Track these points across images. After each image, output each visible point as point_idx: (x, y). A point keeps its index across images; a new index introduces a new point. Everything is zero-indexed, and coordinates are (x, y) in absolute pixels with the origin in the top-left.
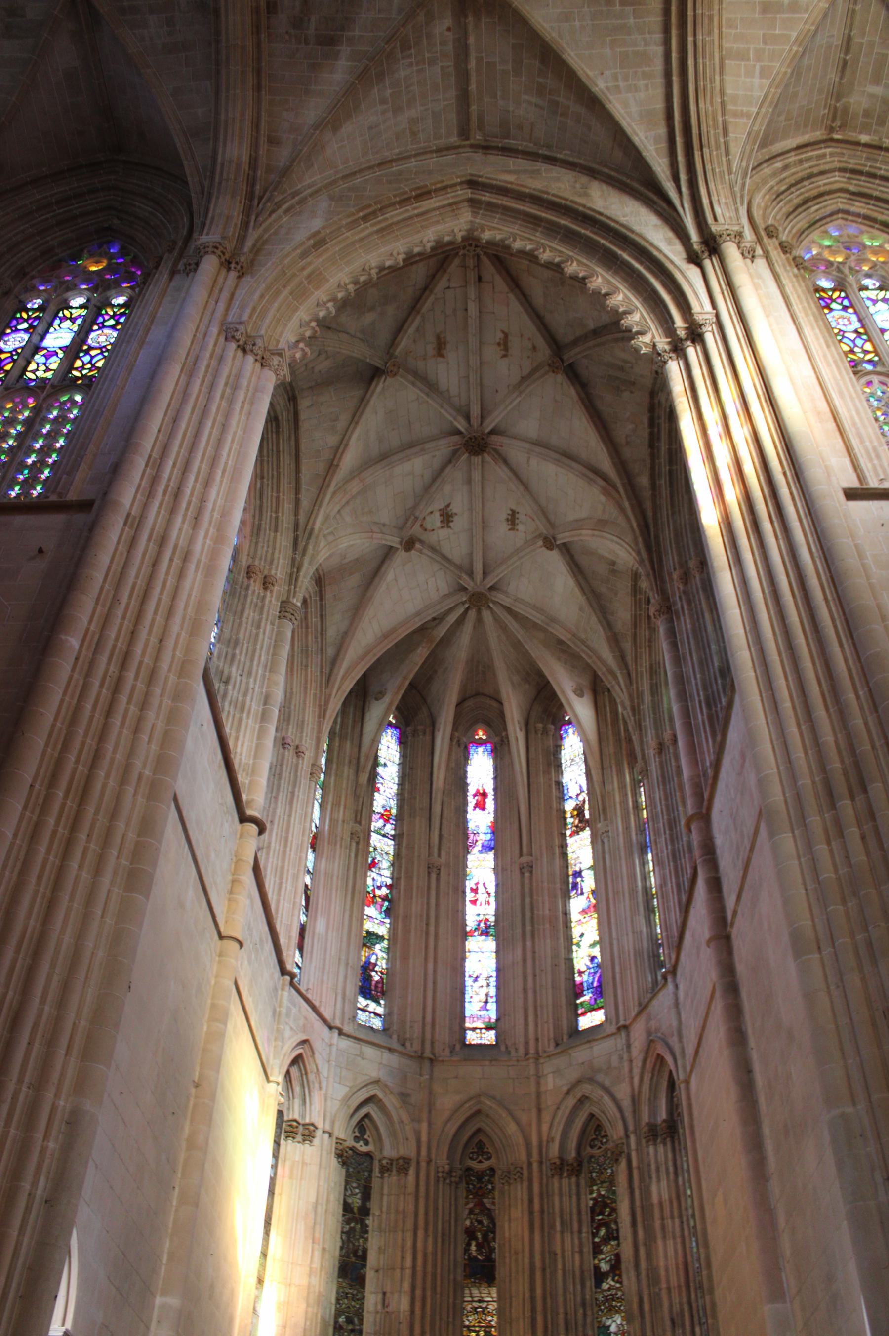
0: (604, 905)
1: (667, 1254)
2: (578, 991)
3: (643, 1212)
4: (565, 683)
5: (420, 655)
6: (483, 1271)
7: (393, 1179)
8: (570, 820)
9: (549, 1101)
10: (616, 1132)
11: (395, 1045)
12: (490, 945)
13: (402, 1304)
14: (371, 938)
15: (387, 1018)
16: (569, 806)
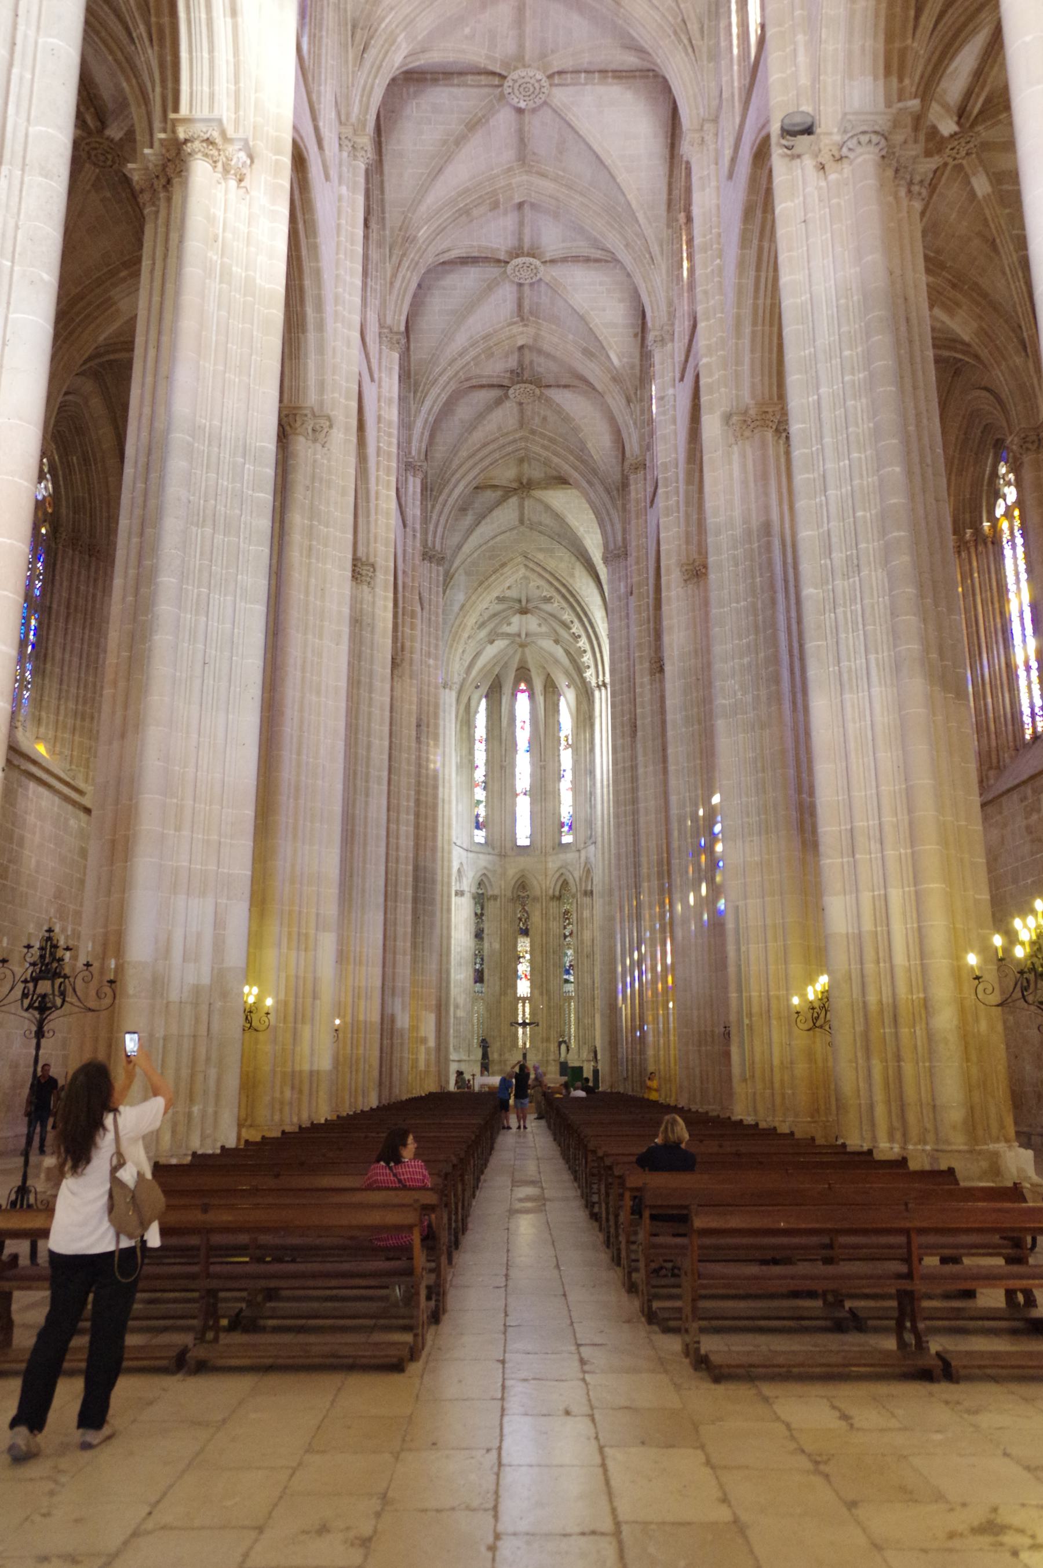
0: (575, 789)
1: (587, 935)
2: (562, 825)
3: (580, 920)
4: (562, 682)
5: (497, 670)
6: (525, 933)
7: (492, 902)
8: (563, 743)
9: (550, 873)
10: (574, 890)
11: (490, 850)
12: (527, 799)
13: (496, 946)
14: (479, 802)
15: (486, 838)
16: (562, 735)
